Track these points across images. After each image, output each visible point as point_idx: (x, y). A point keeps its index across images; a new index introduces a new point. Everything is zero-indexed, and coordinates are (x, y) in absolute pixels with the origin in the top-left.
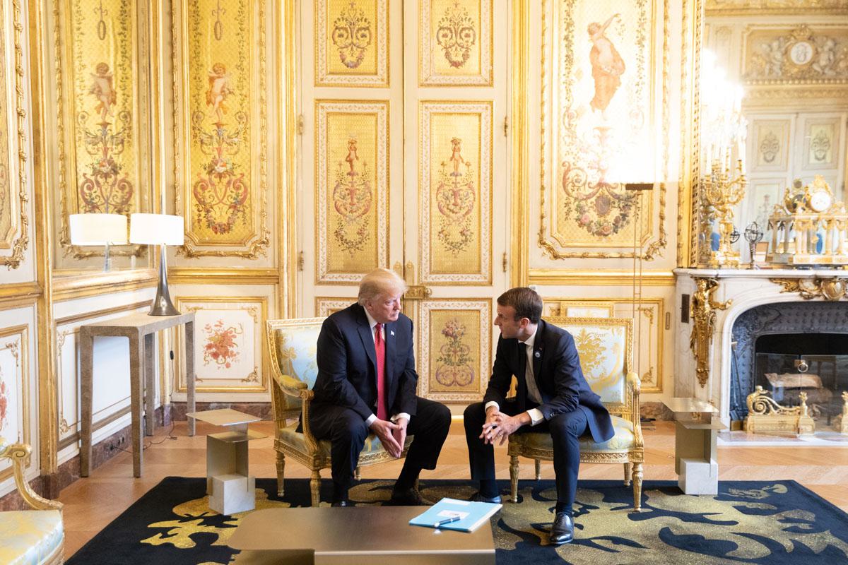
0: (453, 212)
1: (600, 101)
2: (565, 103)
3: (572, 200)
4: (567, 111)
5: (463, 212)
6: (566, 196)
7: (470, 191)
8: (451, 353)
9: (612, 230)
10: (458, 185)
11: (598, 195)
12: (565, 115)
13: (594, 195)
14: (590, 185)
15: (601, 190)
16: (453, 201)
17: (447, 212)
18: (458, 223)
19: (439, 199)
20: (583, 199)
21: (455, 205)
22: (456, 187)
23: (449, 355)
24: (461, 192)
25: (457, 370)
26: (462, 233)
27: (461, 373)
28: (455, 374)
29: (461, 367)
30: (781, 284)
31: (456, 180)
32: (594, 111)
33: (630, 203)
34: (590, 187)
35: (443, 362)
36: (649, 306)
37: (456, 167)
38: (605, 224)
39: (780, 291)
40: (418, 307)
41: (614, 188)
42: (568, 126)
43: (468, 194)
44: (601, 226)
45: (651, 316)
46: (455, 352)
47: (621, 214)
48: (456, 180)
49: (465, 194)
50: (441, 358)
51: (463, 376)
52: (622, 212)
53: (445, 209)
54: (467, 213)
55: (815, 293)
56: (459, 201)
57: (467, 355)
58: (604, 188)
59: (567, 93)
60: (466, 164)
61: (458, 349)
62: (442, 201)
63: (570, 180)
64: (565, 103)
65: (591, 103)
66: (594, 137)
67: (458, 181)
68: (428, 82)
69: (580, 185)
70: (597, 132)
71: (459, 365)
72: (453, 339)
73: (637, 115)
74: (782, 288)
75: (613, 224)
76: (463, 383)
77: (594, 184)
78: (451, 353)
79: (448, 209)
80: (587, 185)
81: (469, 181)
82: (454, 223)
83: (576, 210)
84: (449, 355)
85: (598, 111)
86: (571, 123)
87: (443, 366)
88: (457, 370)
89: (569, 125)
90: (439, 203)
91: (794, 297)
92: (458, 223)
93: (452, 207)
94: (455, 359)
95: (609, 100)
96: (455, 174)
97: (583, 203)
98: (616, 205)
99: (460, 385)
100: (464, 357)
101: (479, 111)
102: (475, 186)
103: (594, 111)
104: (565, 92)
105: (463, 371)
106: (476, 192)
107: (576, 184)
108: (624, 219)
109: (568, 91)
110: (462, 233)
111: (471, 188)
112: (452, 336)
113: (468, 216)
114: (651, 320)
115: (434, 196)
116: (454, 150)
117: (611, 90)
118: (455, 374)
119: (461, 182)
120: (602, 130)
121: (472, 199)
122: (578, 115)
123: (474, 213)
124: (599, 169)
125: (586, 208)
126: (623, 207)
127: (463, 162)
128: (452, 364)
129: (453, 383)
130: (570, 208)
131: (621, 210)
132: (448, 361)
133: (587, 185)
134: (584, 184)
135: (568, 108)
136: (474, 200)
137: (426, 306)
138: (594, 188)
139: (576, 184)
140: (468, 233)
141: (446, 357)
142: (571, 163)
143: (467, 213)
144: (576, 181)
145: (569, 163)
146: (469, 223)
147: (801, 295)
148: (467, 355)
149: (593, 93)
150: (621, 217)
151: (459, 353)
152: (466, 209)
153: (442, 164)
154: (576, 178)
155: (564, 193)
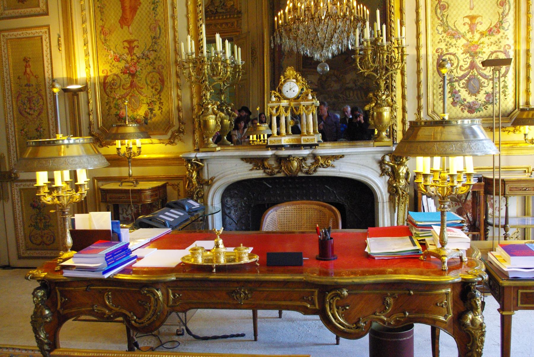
0: (29, 114)
1: (126, 19)
2: (101, 23)
3: (111, 99)
4: (102, 29)
5: (36, 114)
6: (107, 97)
7: (40, 97)
8: (38, 221)
9: (143, 122)
10: (31, 94)
11: (130, 94)
12: (101, 32)
13: (128, 95)
14: (125, 87)
15: (132, 90)
16: (28, 106)
17: (26, 115)
18: (33, 122)
19: (19, 104)
20: (119, 99)
21: (30, 109)
22: (30, 95)
23: (36, 223)
24: (34, 99)
25: (43, 233)
26: (37, 130)
27: (46, 235)
28: (42, 237)
29: (46, 231)
30: (251, 163)
31: (29, 89)
32: (122, 28)
33: (155, 100)
34: (124, 89)
35: (33, 228)
36: (176, 182)
37: (29, 80)
38: (138, 117)
39: (251, 168)
40: (11, 187)
41: (142, 88)
42: (104, 41)
43: (38, 100)
44: (135, 119)
45: (178, 190)
46: (41, 220)
47: (149, 109)
48: (29, 89)
49: (37, 99)
50: (31, 224)
51: (47, 237)
52: (150, 107)
53: (23, 112)
54: (39, 114)
55: (277, 170)
56: (32, 105)
57: (49, 222)
58: (135, 89)
59: (101, 15)
60: (35, 77)
61: (42, 218)
62: (21, 106)
63: (108, 84)
64: (101, 23)
65: (119, 22)
66: (124, 48)
67: (30, 90)
68: (4, 16)
69: (116, 87)
70: (126, 44)
71: (44, 230)
72: (38, 210)
73: (155, 28)
74: (250, 166)
75: (144, 117)
76: (48, 243)
77: (129, 85)
78: (38, 221)
79: (25, 112)
80: (121, 87)
81: (39, 89)
82: (30, 123)
83: (115, 108)
84: (36, 223)
85: (125, 27)
86: (106, 38)
87: (33, 230)
88: (43, 233)
89: (105, 40)
90: (19, 108)
91: (259, 174)
92: (33, 122)
93: (28, 110)
94: (41, 225)
95: (132, 18)
96: (28, 85)
97: (120, 102)
98: (145, 102)
99: (46, 244)
100: (47, 224)
101: (41, 34)
102: (43, 94)
103: (122, 28)
104: (99, 13)
105: (47, 234)
106: (44, 98)
107: (113, 87)
108: (152, 113)
109: (102, 12)
110: (37, 130)
111: (40, 95)
112: (37, 208)
113: (40, 116)
114: (178, 193)
115: (14, 103)
116: (26, 67)
117: (134, 10)
118: (42, 237)
119: (33, 90)
120: (130, 42)
121: (41, 103)
122: (110, 31)
123: (43, 115)
124: (130, 74)
125: (122, 106)
126: (150, 103)
127: (33, 75)
128: (40, 229)
129: (41, 243)
130: (110, 106)
131: (149, 106)
132: (36, 227)
133: (121, 87)
134: (119, 86)
135: (103, 27)
136: (43, 104)
137: (17, 185)
138: (127, 89)
139: (113, 87)
140: (42, 129)
141: (35, 224)
142: (108, 70)
143: (39, 114)
144: (113, 85)
145: (107, 71)
146: (41, 122)
147: (265, 172)
148: (49, 222)
149: (120, 14)
150: (149, 111)
151: (43, 221)
152: (38, 111)
153: (19, 78)
154: (112, 82)
155: (105, 95)
